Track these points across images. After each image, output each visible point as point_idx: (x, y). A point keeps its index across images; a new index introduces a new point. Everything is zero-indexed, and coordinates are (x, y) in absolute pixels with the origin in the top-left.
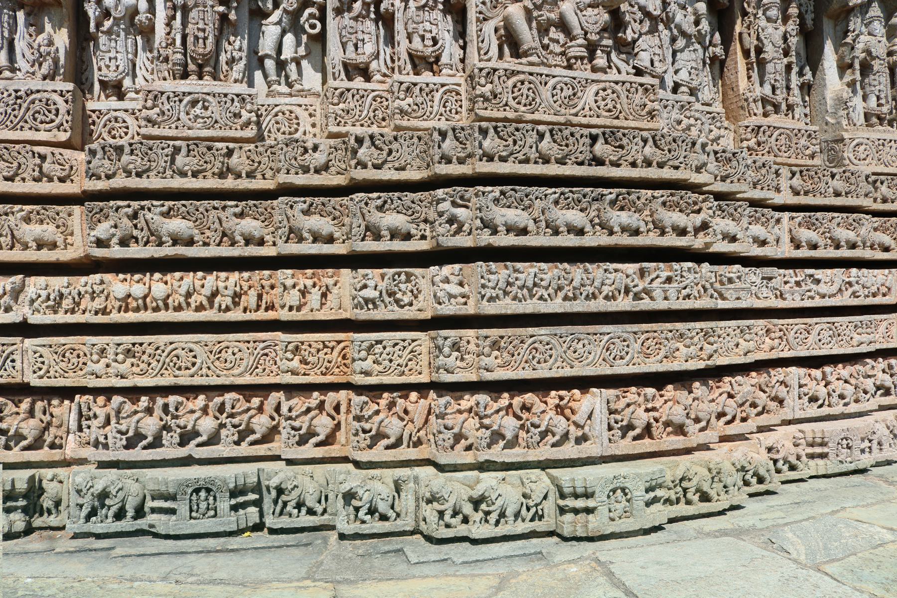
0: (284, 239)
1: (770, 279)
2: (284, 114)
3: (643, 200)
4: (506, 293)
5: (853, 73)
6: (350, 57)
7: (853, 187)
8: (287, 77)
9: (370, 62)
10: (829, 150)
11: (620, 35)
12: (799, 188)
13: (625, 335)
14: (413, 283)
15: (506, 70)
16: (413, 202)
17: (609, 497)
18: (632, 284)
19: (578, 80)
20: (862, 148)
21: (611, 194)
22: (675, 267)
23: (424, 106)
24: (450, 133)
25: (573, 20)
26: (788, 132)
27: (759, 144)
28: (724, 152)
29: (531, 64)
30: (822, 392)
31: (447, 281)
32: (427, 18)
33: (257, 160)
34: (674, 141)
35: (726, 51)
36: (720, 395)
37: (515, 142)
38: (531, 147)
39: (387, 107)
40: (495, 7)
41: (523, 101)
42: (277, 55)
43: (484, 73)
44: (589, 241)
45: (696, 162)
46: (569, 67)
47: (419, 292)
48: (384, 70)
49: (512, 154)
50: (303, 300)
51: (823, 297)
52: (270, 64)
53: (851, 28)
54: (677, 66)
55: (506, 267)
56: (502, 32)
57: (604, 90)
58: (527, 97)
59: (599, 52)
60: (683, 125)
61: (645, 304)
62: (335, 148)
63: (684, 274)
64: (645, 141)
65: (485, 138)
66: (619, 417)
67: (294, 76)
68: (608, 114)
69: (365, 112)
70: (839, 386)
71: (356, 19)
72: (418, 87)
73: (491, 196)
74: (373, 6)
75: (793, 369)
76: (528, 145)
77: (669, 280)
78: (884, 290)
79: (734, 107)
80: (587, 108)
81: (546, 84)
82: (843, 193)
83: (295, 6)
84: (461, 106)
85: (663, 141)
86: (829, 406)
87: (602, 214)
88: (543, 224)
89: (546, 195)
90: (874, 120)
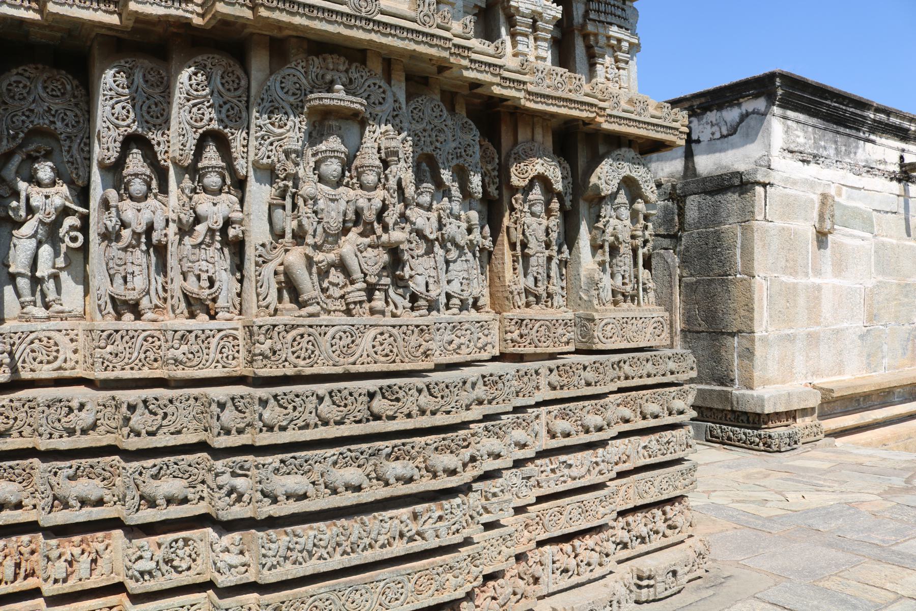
0: (48, 509)
2: (40, 340)
3: (417, 449)
4: (286, 558)
5: (604, 254)
6: (118, 292)
8: (44, 296)
9: (141, 298)
10: (582, 326)
11: (398, 273)
12: (556, 384)
13: (399, 578)
14: (191, 547)
15: (285, 325)
16: (190, 465)
18: (406, 529)
19: (356, 327)
20: (610, 326)
22: (446, 507)
23: (200, 354)
24: (229, 404)
25: (353, 263)
26: (548, 323)
27: (521, 336)
28: (491, 375)
29: (311, 315)
30: (572, 563)
31: (227, 550)
32: (204, 257)
33: (12, 415)
35: (494, 242)
37: (295, 408)
38: (311, 413)
39: (160, 347)
40: (275, 248)
41: (302, 356)
42: (31, 272)
43: (263, 330)
44: (365, 497)
46: (348, 312)
47: (198, 555)
48: (156, 301)
49: (292, 421)
50: (70, 569)
52: (23, 283)
53: (603, 214)
54: (451, 276)
55: (286, 533)
56: (282, 278)
57: (382, 334)
58: (307, 350)
59: (377, 293)
60: (454, 346)
61: (419, 545)
62: (104, 405)
63: (454, 511)
64: (420, 391)
65: (265, 407)
67: (51, 296)
69: (136, 354)
70: (585, 555)
71: (125, 250)
72: (193, 335)
74: (144, 236)
75: (547, 548)
76: (307, 411)
77: (440, 518)
78: (624, 458)
79: (500, 299)
80: (365, 354)
81: (325, 334)
83: (54, 217)
84: (238, 352)
85: (437, 388)
86: (578, 574)
87: (378, 468)
88: (323, 486)
89: (325, 458)
90: (620, 297)
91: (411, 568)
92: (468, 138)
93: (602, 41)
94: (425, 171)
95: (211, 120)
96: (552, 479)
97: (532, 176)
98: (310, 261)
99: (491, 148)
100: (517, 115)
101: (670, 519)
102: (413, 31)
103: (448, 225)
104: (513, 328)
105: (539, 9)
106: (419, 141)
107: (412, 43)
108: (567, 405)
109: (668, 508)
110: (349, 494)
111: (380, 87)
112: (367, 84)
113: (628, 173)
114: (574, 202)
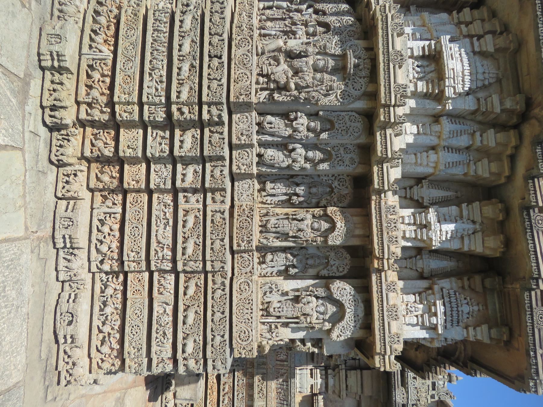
1: (164, 184)
17: (58, 35)
20: (247, 287)
21: (197, 63)
28: (224, 143)
30: (106, 229)
36: (106, 139)
37: (218, 26)
44: (175, 53)
45: (212, 110)
51: (157, 232)
57: (248, 78)
59: (266, 80)
60: (240, 136)
61: (147, 77)
66: (98, 64)
68: (236, 77)
70: (108, 240)
73: (195, 14)
77: (157, 90)
78: (161, 290)
82: (212, 246)
90: (266, 306)
91: (137, 73)
92: (347, 162)
93: (431, 299)
95: (335, 27)
96: (160, 213)
98: (279, 50)
99: (346, 202)
100: (368, 216)
101: (109, 337)
102: (390, 82)
105: (433, 227)
109: (118, 336)
110: (178, 47)
111: (361, 88)
112: (361, 81)
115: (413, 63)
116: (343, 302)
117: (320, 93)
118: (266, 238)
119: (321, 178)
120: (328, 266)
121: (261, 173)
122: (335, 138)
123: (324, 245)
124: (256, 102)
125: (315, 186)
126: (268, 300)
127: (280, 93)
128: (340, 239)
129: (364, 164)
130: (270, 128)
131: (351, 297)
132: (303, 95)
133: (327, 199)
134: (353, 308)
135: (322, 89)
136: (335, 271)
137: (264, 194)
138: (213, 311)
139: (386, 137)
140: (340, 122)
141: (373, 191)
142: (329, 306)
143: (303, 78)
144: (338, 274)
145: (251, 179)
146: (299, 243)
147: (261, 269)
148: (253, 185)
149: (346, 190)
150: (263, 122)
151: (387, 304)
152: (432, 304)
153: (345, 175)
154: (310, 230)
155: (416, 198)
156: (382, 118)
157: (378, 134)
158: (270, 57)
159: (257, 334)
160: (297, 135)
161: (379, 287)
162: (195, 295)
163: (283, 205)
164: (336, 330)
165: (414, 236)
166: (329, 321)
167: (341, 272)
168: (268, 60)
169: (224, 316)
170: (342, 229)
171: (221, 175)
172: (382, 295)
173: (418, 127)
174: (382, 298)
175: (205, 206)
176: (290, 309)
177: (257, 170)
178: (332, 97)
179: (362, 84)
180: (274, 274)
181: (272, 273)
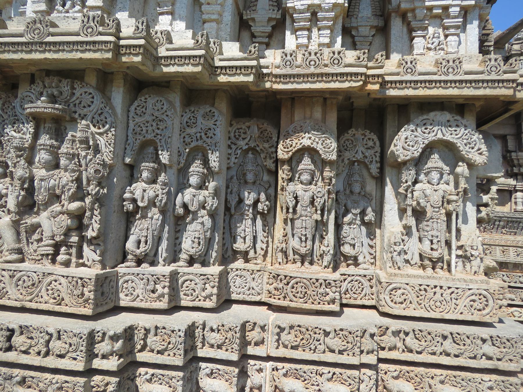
7: (350, 346)
12: (287, 343)
20: (400, 292)
26: (305, 281)
28: (164, 328)
34: (75, 336)
45: (101, 352)
53: (404, 178)
57: (56, 281)
60: (156, 295)
68: (52, 301)
82: (337, 351)
90: (427, 262)
92: (210, 124)
93: (421, 13)
94: (149, 153)
97: (296, 149)
98: (16, 224)
99: (271, 129)
103: (160, 196)
104: (271, 281)
106: (142, 130)
107: (78, 53)
108: (301, 366)
111: (90, 94)
113: (440, 136)
114: (382, 170)
115: (59, 12)
116: (426, 142)
117: (91, 160)
118: (321, 256)
119: (232, 164)
120: (364, 163)
121: (219, 258)
122: (169, 140)
123: (335, 167)
124: (99, 266)
125: (245, 175)
126: (416, 259)
127: (88, 226)
128: (328, 141)
129: (214, 99)
130: (146, 244)
131: (419, 130)
132: (93, 189)
133: (265, 158)
134: (436, 129)
135: (85, 157)
136: (373, 152)
137: (251, 254)
138: (441, 354)
139: (171, 57)
140: (144, 131)
141: (258, 86)
142: (430, 164)
143: (63, 187)
144: (378, 149)
145: (228, 273)
146: (332, 205)
147: (365, 263)
148: (237, 270)
149: (253, 128)
150: (135, 256)
151: (435, 74)
152: (429, 13)
153: (230, 129)
154: (312, 186)
155: (269, 29)
156: (138, 59)
157: (165, 70)
158: (27, 240)
159: (477, 282)
160: (161, 201)
161: (408, 85)
162: (413, 381)
163: (271, 224)
164: (470, 156)
165: (329, 32)
166: (456, 166)
167: (375, 143)
168: (32, 243)
169: (450, 336)
170: (313, 138)
171: (219, 330)
172: (421, 82)
173: (162, 14)
174: (425, 81)
175: (269, 358)
176: (435, 225)
177: (214, 265)
178: (102, 141)
179: (84, 92)
180: (371, 243)
181: (371, 247)
